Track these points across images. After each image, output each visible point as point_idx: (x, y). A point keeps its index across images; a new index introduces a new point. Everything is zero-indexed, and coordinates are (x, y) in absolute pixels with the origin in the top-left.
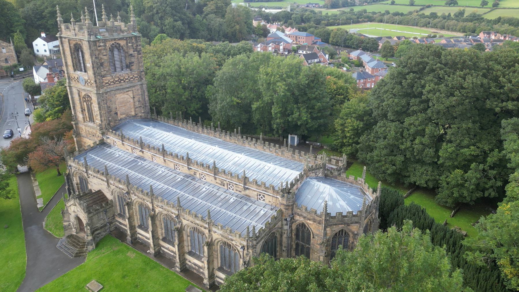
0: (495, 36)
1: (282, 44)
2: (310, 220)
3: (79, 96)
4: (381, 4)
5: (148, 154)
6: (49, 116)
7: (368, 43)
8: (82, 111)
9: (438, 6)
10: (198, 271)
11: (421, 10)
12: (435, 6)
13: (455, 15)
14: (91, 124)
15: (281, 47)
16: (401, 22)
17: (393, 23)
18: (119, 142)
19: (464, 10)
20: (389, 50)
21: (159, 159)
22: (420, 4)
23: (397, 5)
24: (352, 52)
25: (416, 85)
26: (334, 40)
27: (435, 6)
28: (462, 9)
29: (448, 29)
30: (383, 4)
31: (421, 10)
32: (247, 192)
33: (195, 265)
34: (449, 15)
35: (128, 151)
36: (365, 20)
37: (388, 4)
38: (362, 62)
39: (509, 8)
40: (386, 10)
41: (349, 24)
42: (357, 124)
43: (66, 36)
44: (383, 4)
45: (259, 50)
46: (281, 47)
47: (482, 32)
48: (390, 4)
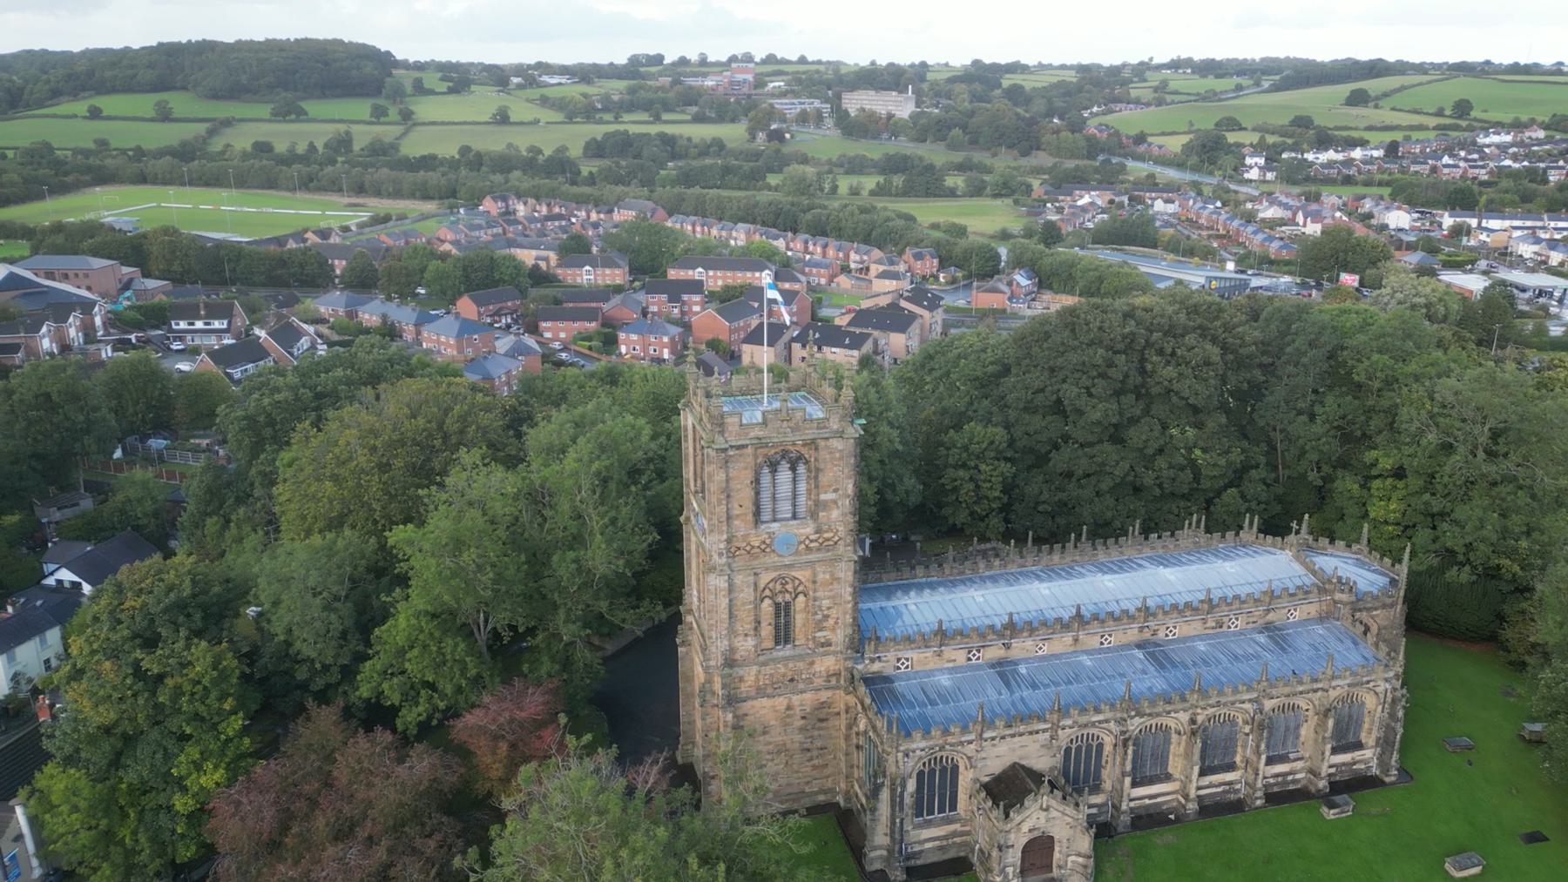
0: (525, 204)
1: (96, 309)
2: (1376, 609)
3: (755, 590)
4: (47, 116)
5: (1023, 647)
6: (198, 767)
7: (302, 266)
8: (756, 629)
9: (251, 120)
10: (1287, 783)
11: (212, 133)
12: (242, 120)
13: (326, 146)
14: (787, 651)
15: (98, 321)
16: (217, 179)
17: (207, 184)
18: (919, 658)
19: (347, 133)
20: (403, 280)
21: (1061, 644)
22: (191, 116)
23: (109, 118)
24: (363, 303)
25: (1131, 373)
26: (176, 267)
27: (242, 120)
28: (342, 128)
29: (378, 193)
30: (55, 116)
31: (212, 133)
32: (1271, 617)
33: (1277, 776)
34: (312, 148)
35: (951, 665)
36: (82, 178)
37: (75, 116)
38: (393, 323)
39: (443, 123)
40: (96, 136)
41: (40, 197)
42: (1005, 468)
43: (744, 442)
44: (55, 116)
45: (46, 344)
46: (98, 321)
47: (488, 198)
48: (84, 118)
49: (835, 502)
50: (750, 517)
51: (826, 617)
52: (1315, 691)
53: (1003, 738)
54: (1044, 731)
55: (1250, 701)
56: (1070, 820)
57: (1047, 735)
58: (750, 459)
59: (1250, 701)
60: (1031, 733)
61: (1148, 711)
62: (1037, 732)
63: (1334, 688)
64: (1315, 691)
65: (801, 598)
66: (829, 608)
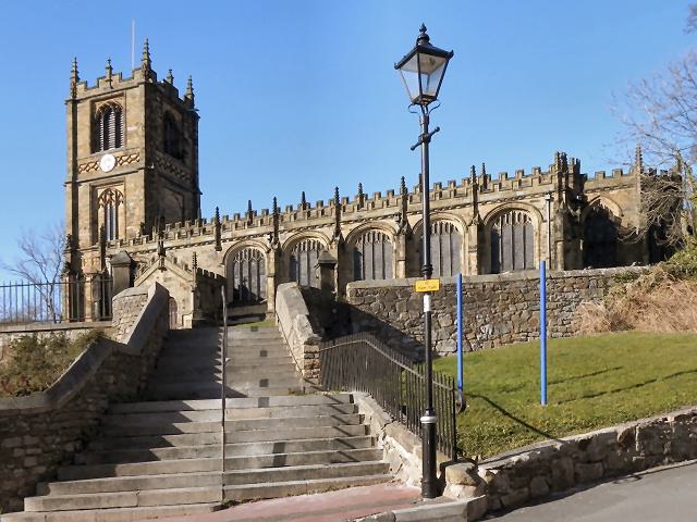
49: (136, 132)
50: (88, 146)
51: (133, 215)
52: (464, 206)
53: (178, 247)
54: (210, 243)
55: (392, 216)
56: (184, 282)
57: (214, 245)
58: (88, 109)
59: (392, 216)
60: (199, 244)
61: (295, 226)
62: (204, 243)
63: (484, 203)
64: (464, 206)
65: (121, 205)
66: (134, 208)
